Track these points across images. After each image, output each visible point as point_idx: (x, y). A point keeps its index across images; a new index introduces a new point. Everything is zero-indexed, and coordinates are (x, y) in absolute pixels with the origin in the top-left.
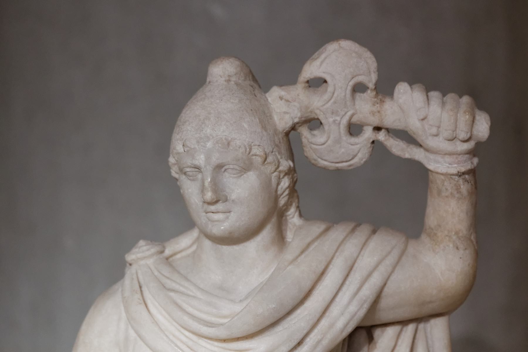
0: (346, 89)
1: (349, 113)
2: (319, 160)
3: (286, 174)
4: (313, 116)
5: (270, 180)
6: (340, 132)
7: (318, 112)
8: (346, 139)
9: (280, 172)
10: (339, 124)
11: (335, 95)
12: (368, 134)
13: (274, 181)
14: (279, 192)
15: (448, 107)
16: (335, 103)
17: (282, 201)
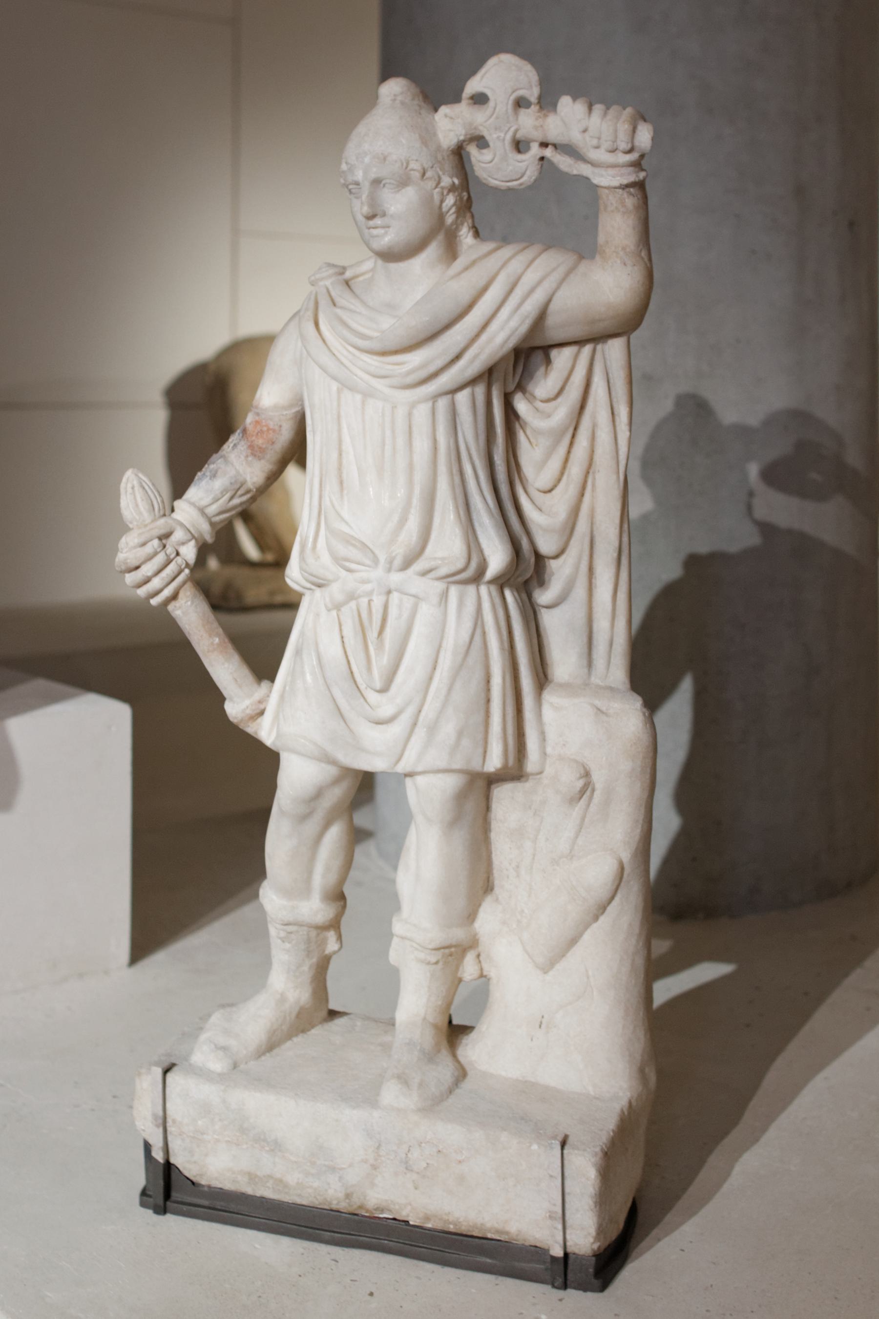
0: (507, 103)
1: (513, 129)
3: (450, 191)
4: (477, 133)
5: (432, 196)
6: (505, 151)
7: (481, 128)
8: (514, 156)
9: (443, 188)
10: (504, 140)
11: (497, 110)
12: (535, 150)
13: (437, 198)
14: (444, 209)
15: (609, 117)
16: (497, 118)
17: (450, 219)
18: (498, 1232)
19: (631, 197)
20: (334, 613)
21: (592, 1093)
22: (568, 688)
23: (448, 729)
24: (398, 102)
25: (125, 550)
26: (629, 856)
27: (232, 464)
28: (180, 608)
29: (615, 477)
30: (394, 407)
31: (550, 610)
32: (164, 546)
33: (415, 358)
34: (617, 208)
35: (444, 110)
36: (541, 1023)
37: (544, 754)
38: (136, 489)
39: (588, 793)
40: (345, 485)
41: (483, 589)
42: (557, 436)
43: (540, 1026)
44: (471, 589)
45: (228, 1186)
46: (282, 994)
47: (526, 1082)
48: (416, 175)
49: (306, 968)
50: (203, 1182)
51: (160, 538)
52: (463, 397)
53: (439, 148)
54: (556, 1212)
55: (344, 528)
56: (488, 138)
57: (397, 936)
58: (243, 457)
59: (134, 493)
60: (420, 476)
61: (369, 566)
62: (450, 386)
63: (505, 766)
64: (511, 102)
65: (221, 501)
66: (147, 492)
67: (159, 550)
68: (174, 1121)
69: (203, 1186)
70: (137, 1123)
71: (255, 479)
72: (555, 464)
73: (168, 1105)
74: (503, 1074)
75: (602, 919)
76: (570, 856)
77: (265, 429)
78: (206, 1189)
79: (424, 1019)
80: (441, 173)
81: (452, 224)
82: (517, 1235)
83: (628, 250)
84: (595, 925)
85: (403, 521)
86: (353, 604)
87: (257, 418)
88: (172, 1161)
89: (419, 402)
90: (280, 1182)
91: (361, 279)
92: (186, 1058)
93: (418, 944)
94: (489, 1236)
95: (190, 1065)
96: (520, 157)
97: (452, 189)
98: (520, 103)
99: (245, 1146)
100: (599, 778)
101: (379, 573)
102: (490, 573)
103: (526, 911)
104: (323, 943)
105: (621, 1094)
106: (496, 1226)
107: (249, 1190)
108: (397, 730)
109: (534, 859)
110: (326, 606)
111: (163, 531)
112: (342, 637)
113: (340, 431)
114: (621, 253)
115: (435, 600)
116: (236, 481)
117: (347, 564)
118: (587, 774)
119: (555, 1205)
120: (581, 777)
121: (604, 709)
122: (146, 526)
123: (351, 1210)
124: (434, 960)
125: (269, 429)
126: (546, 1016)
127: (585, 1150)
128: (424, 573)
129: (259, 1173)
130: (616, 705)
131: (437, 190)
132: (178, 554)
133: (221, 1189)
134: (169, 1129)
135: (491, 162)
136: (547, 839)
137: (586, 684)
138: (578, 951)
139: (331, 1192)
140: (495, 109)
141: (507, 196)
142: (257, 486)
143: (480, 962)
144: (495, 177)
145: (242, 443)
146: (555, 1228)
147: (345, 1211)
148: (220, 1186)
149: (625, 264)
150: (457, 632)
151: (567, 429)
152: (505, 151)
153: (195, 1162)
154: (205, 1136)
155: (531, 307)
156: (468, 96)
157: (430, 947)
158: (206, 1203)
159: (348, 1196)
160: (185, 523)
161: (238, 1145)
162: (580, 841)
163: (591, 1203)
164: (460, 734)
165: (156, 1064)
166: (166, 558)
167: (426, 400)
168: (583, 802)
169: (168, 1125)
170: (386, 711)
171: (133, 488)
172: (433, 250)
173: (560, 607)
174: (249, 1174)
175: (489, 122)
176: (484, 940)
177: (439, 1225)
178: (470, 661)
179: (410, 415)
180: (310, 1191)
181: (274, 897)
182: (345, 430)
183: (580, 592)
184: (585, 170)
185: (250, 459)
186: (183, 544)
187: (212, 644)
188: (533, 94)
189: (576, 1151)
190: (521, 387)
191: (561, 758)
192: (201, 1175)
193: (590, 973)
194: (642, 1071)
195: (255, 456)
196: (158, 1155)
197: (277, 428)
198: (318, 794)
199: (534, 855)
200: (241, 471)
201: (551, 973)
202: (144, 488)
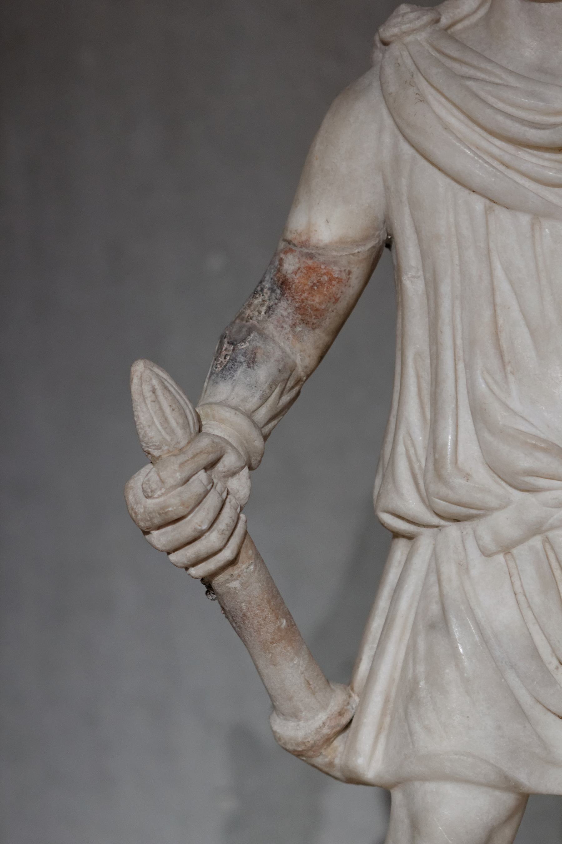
38: (159, 392)
59: (156, 400)
66: (174, 397)
77: (326, 278)
87: (310, 262)
116: (284, 367)
145: (283, 304)
160: (230, 440)
171: (154, 391)
185: (299, 329)
187: (279, 628)
197: (344, 276)
200: (288, 350)
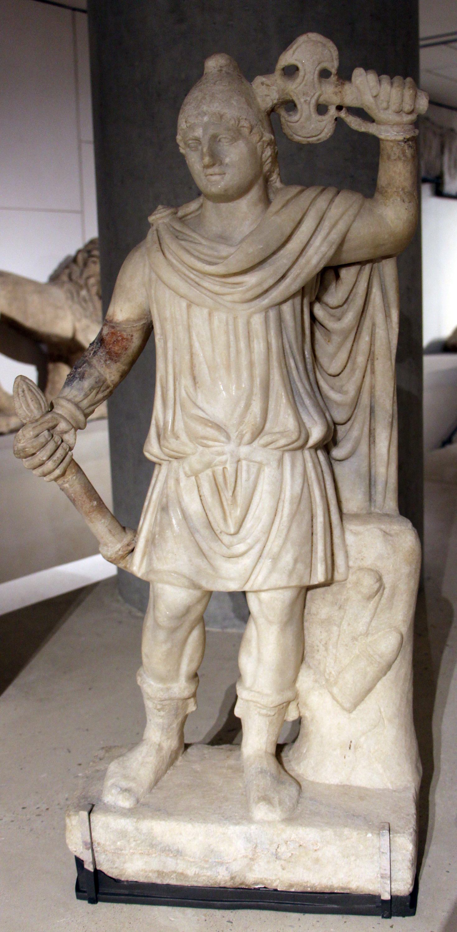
0: (314, 73)
1: (317, 94)
2: (294, 135)
3: (268, 144)
4: (288, 98)
5: (256, 148)
6: (310, 111)
7: (292, 94)
8: (315, 116)
9: (264, 142)
10: (309, 103)
11: (306, 79)
12: (332, 111)
13: (259, 150)
14: (264, 160)
15: (395, 84)
16: (305, 85)
17: (266, 168)
18: (342, 888)
19: (410, 148)
20: (193, 478)
21: (391, 788)
22: (356, 516)
23: (288, 558)
24: (224, 72)
25: (22, 441)
26: (406, 629)
27: (95, 368)
28: (68, 481)
29: (389, 363)
30: (235, 318)
31: (342, 462)
32: (52, 436)
33: (251, 279)
34: (399, 157)
35: (259, 79)
36: (350, 746)
37: (348, 567)
38: (26, 392)
39: (381, 591)
40: (198, 379)
41: (307, 453)
42: (345, 334)
43: (350, 748)
44: (299, 453)
45: (142, 880)
46: (159, 745)
47: (344, 786)
48: (246, 131)
49: (174, 725)
50: (123, 879)
51: (49, 430)
52: (287, 308)
53: (259, 110)
54: (386, 874)
55: (201, 414)
56: (297, 102)
57: (242, 699)
58: (102, 362)
59: (24, 396)
60: (258, 371)
61: (223, 442)
62: (279, 300)
63: (326, 580)
64: (317, 72)
65: (90, 397)
66: (34, 394)
67: (49, 439)
68: (99, 844)
69: (123, 881)
70: (70, 847)
71: (113, 378)
72: (343, 355)
73: (93, 834)
74: (327, 782)
75: (389, 673)
76: (367, 634)
77: (120, 338)
78: (125, 883)
79: (266, 752)
80: (262, 130)
81: (268, 172)
82: (356, 890)
83: (406, 190)
84: (384, 678)
85: (248, 406)
86: (209, 472)
87: (113, 330)
88: (98, 868)
89: (255, 313)
90: (182, 875)
91: (189, 217)
92: (99, 799)
93: (261, 704)
94: (336, 891)
95: (105, 804)
96: (320, 118)
97: (270, 143)
98: (324, 74)
99: (154, 855)
100: (388, 580)
101: (229, 448)
102: (311, 442)
103: (333, 673)
104: (186, 706)
105: (409, 785)
106: (341, 885)
107: (159, 881)
108: (247, 561)
109: (339, 638)
110: (186, 474)
111: (51, 425)
112: (200, 496)
113: (190, 338)
114: (401, 193)
115: (274, 464)
116: (99, 380)
117: (205, 442)
118: (380, 579)
119: (385, 870)
120: (377, 582)
121: (388, 531)
122: (37, 421)
123: (234, 886)
124: (273, 714)
125: (123, 339)
126: (353, 741)
127: (404, 833)
128: (266, 446)
129: (165, 871)
130: (395, 527)
131: (259, 144)
132: (62, 441)
133: (136, 882)
134: (95, 849)
135: (297, 121)
136: (349, 624)
137: (370, 514)
138: (373, 696)
139: (220, 877)
140: (304, 77)
141: (310, 150)
142: (114, 383)
143: (299, 708)
144: (300, 133)
145: (101, 350)
146: (385, 883)
147: (231, 887)
148: (135, 880)
149: (404, 201)
150: (291, 487)
151: (353, 328)
152: (310, 111)
153: (116, 868)
154: (123, 851)
155: (335, 236)
156: (282, 67)
157: (271, 706)
158: (126, 892)
159: (232, 878)
160: (65, 416)
161: (148, 855)
162: (373, 624)
163: (409, 864)
164: (296, 561)
165: (83, 809)
166: (55, 445)
167: (260, 312)
168: (377, 598)
169: (94, 847)
170: (241, 548)
171: (23, 391)
172: (255, 193)
173: (349, 460)
174: (158, 871)
175: (299, 88)
176: (302, 693)
177: (300, 889)
178: (302, 507)
179: (248, 323)
180: (204, 878)
181: (152, 683)
182: (194, 337)
183: (364, 448)
184: (371, 129)
185: (108, 362)
186: (66, 432)
187: (92, 506)
188: (333, 66)
189: (399, 835)
190: (318, 299)
191: (361, 569)
192: (121, 875)
193: (382, 710)
194: (417, 767)
195: (112, 360)
196: (89, 867)
197: (129, 337)
198: (188, 610)
199: (339, 635)
200: (102, 372)
201: (354, 712)
202: (32, 391)
